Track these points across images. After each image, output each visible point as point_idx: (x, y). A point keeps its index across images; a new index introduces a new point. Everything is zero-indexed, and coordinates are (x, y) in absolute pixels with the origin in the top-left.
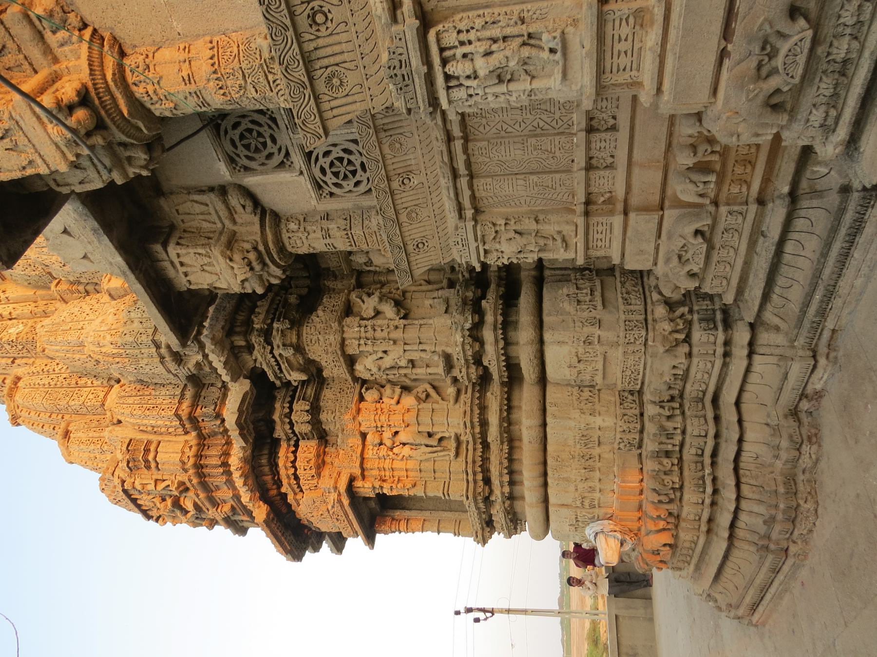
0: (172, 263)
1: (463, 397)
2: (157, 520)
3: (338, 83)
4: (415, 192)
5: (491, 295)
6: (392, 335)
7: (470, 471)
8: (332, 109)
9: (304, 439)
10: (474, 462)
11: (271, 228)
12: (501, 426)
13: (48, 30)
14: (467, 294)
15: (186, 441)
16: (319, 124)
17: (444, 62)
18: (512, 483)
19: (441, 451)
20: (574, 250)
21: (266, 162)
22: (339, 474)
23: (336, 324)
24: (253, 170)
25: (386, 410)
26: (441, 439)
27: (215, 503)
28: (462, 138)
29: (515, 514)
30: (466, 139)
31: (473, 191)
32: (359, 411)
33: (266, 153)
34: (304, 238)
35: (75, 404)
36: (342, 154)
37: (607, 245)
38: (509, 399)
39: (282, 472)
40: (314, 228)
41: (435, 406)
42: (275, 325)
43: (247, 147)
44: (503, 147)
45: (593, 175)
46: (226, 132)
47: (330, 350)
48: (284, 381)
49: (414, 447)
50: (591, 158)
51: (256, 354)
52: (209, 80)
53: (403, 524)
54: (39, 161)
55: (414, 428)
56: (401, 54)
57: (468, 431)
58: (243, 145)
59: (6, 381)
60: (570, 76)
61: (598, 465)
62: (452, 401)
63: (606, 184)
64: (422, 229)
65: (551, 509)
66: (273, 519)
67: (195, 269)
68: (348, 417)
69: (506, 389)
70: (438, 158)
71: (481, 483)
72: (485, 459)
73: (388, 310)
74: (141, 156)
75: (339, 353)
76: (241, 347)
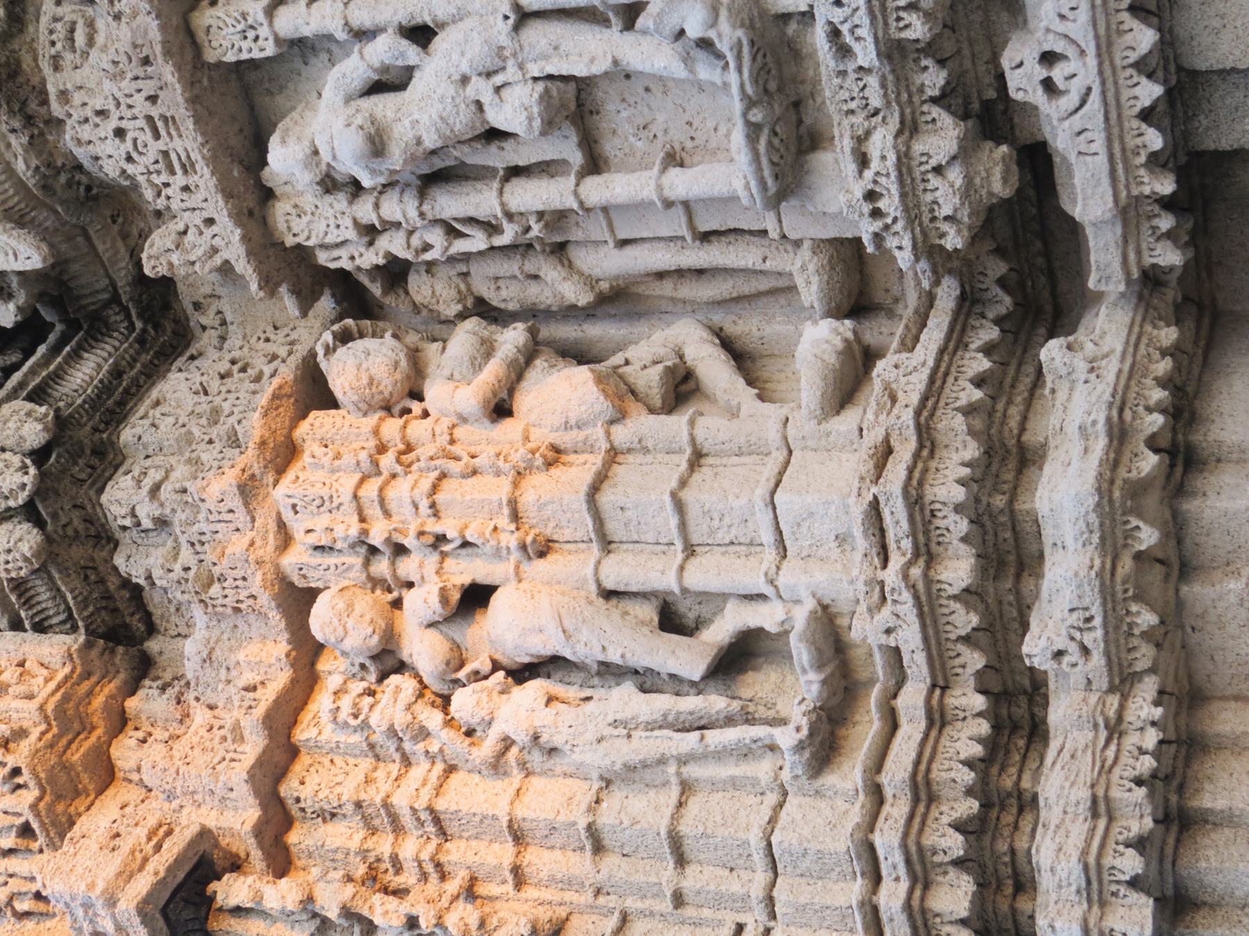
7: (887, 840)
10: (923, 792)
12: (1111, 540)
19: (729, 721)
26: (738, 657)
32: (284, 454)
38: (1185, 407)
55: (575, 565)
68: (220, 487)
69: (1168, 335)
72: (1001, 807)
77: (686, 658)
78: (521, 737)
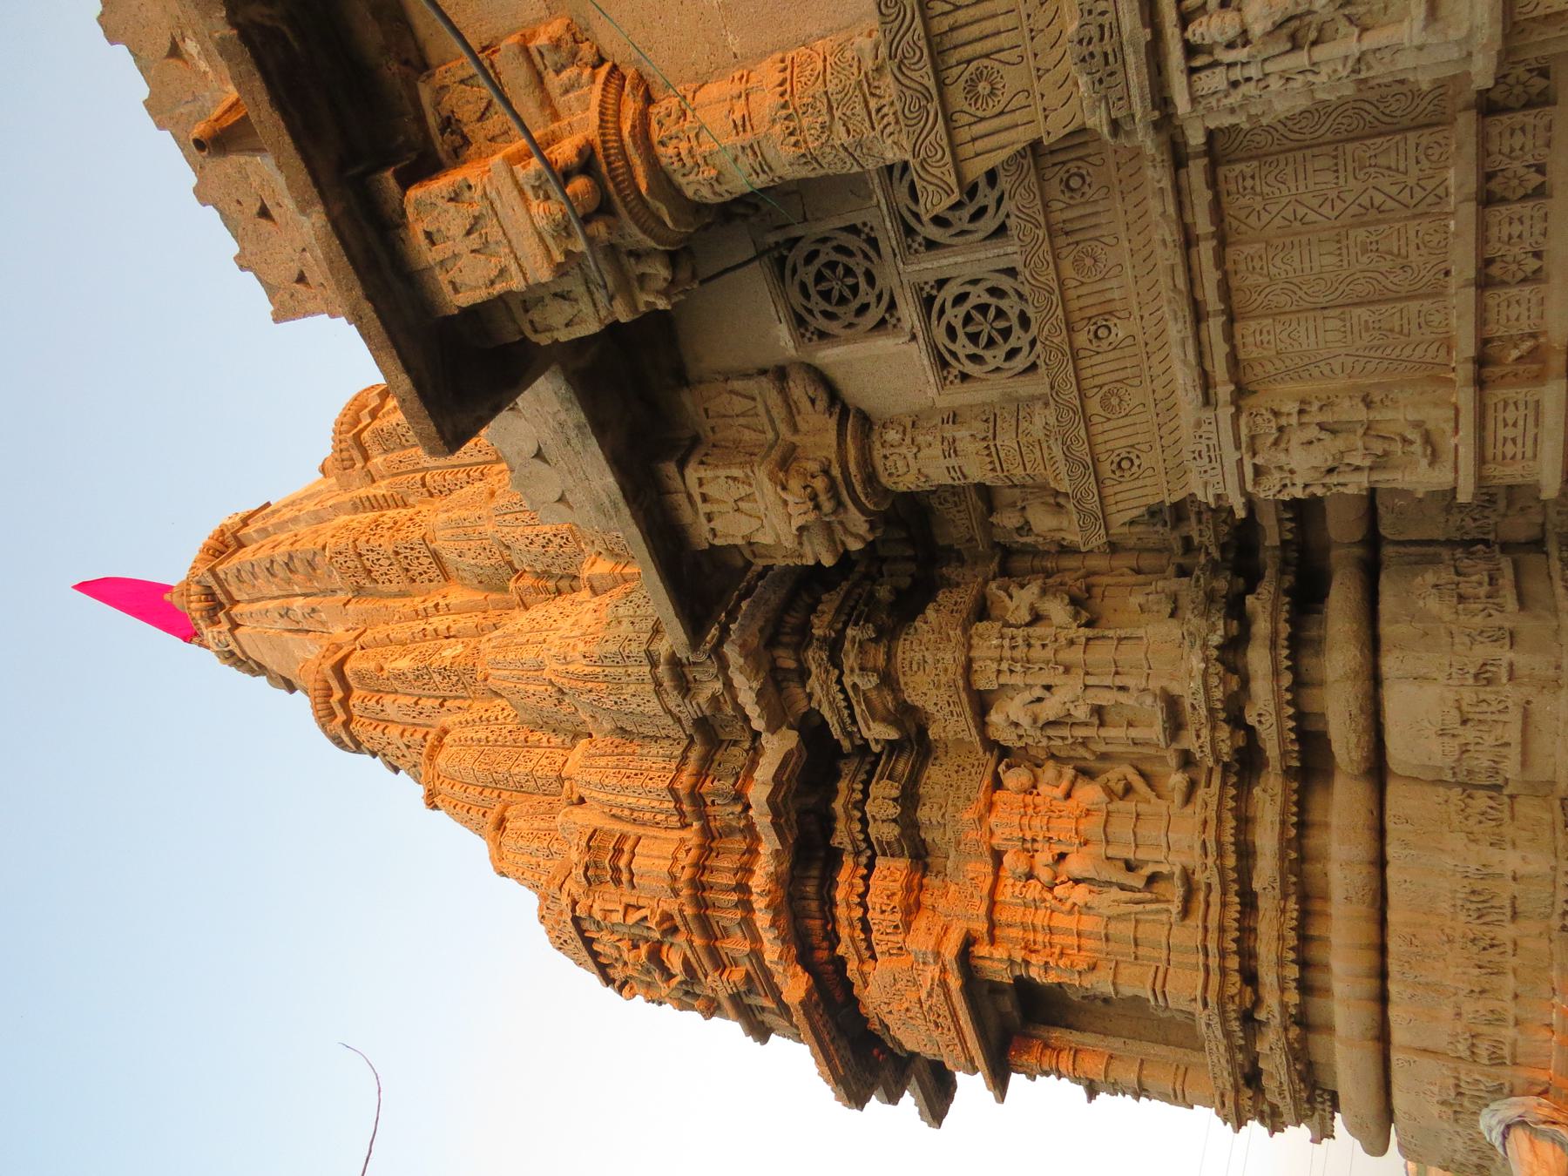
0: (690, 496)
1: (1201, 792)
2: (620, 990)
3: (987, 91)
4: (1118, 353)
5: (1266, 589)
6: (1062, 656)
7: (1212, 947)
8: (974, 140)
9: (884, 854)
10: (1222, 929)
11: (854, 438)
12: (1282, 856)
13: (550, 70)
14: (1215, 584)
15: (682, 840)
16: (950, 166)
17: (1185, 20)
18: (1305, 988)
19: (1151, 901)
20: (1449, 465)
21: (856, 321)
22: (946, 929)
23: (959, 632)
24: (834, 336)
25: (1043, 809)
26: (1152, 879)
27: (720, 964)
28: (1214, 235)
29: (1310, 1065)
30: (1222, 241)
31: (1233, 348)
32: (991, 806)
33: (855, 304)
34: (910, 456)
35: (520, 770)
36: (986, 298)
37: (1529, 454)
38: (1302, 806)
39: (841, 912)
40: (929, 438)
41: (1142, 807)
42: (850, 632)
43: (826, 295)
44: (1296, 253)
45: (1494, 298)
46: (794, 271)
47: (944, 679)
48: (859, 742)
49: (1095, 889)
50: (1489, 262)
51: (813, 684)
52: (774, 121)
53: (1065, 1061)
54: (514, 268)
55: (1099, 849)
56: (1103, 13)
57: (1210, 861)
58: (820, 293)
59: (429, 738)
60: (1443, 12)
61: (1513, 962)
62: (1178, 798)
63: (1523, 318)
64: (1128, 431)
65: (1396, 1057)
66: (817, 1005)
67: (723, 508)
68: (968, 816)
69: (1295, 785)
70: (1164, 282)
71: (1235, 978)
72: (1247, 931)
73: (1058, 611)
74: (659, 271)
75: (961, 683)
76: (788, 670)
77: (1137, 881)
78: (1081, 903)
